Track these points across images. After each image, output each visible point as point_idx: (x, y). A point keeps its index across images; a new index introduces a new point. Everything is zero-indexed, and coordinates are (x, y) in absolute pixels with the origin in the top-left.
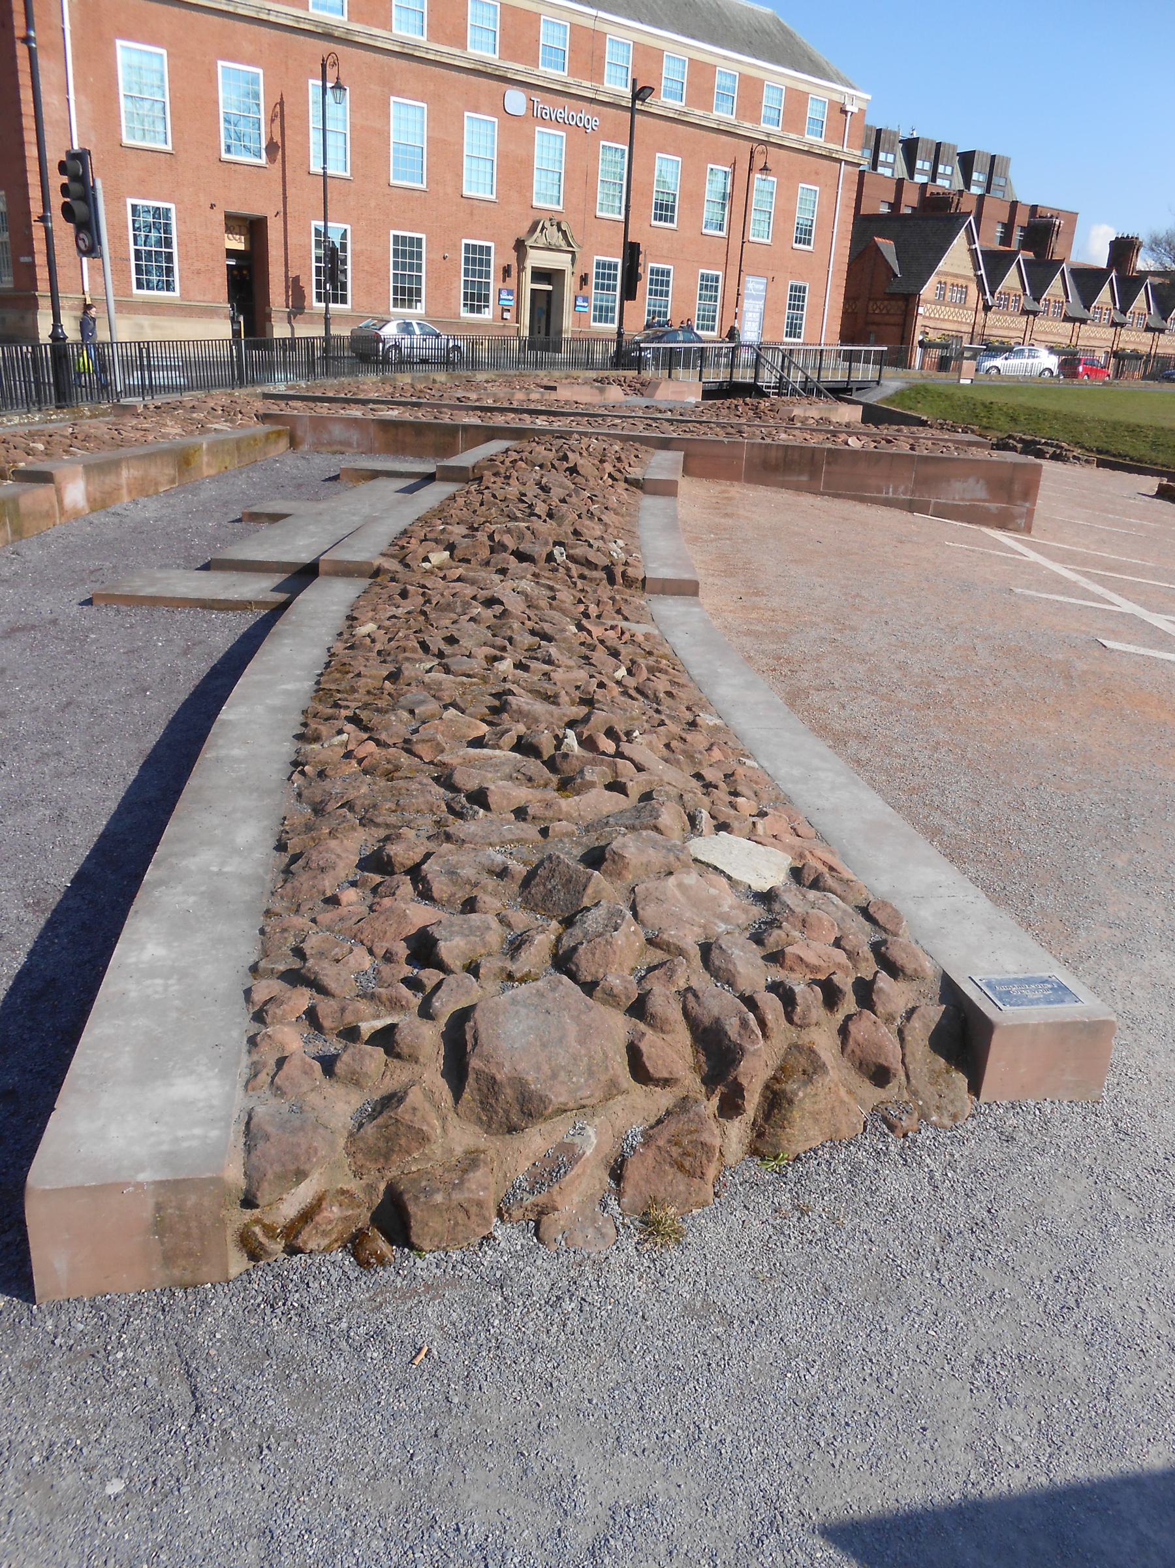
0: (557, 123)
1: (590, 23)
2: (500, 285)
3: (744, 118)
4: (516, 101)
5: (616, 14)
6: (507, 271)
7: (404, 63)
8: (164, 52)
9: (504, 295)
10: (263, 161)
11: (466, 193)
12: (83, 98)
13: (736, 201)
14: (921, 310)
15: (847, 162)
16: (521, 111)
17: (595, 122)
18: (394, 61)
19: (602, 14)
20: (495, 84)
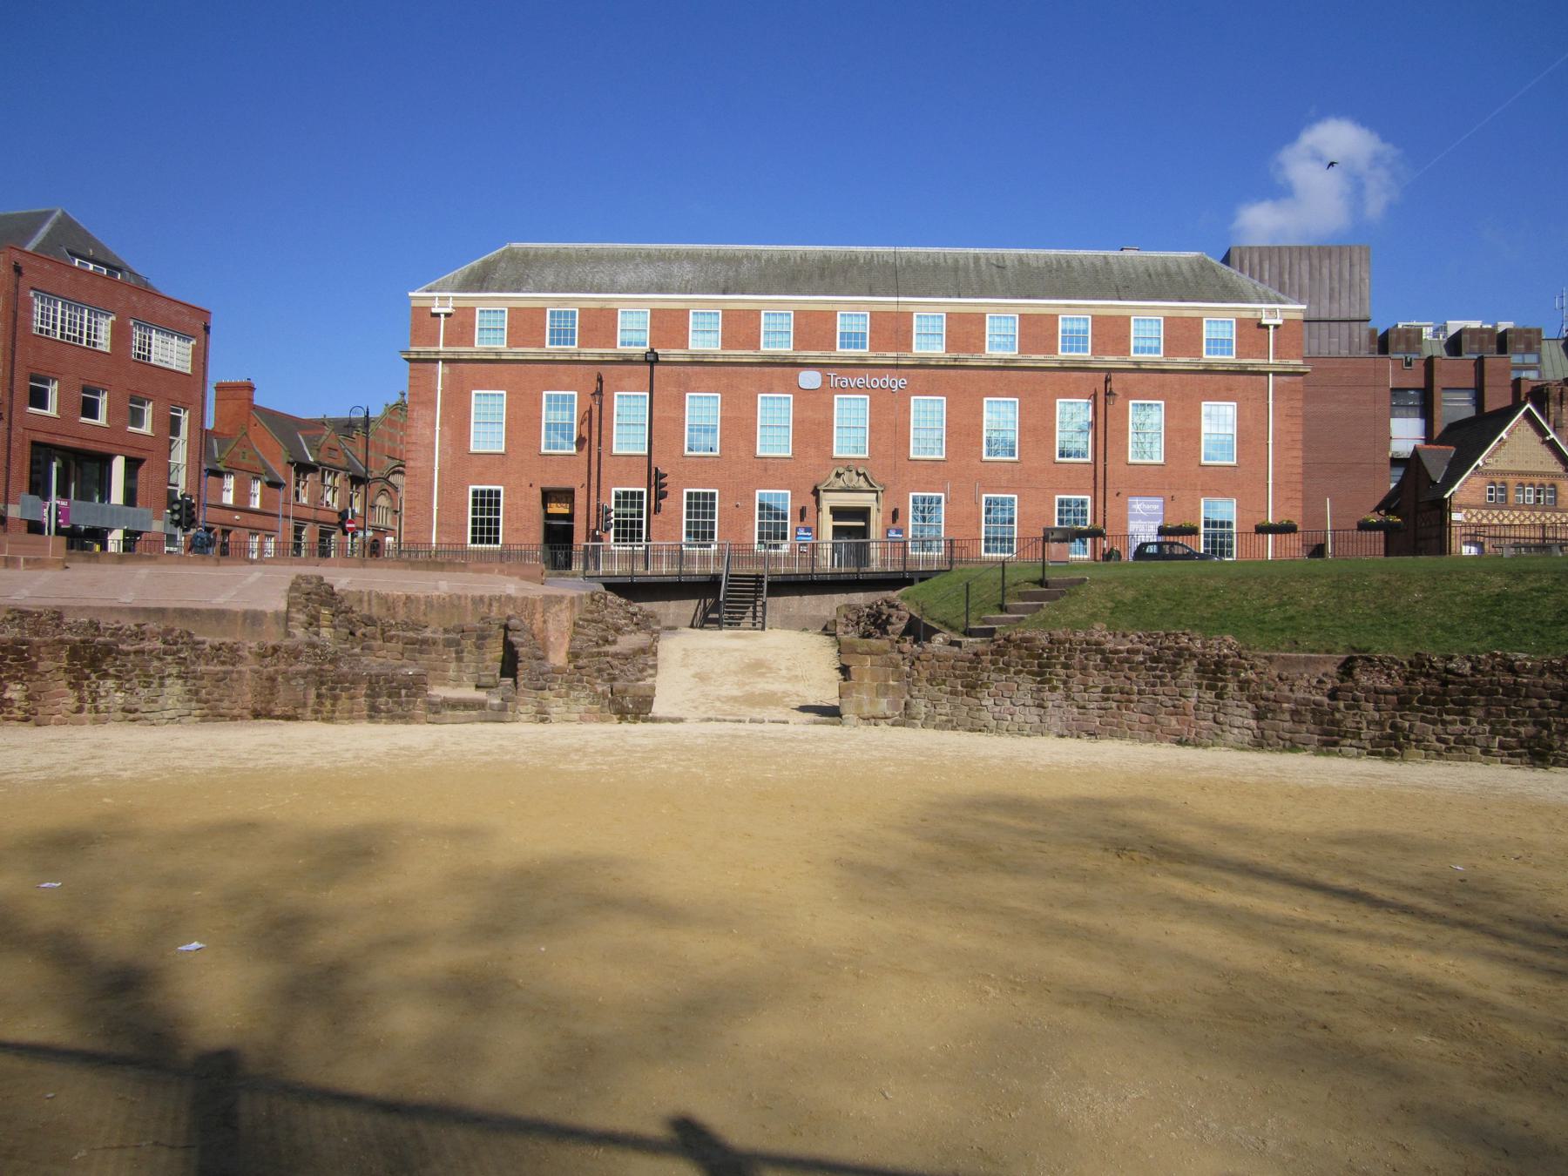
0: (858, 390)
1: (893, 308)
2: (798, 524)
3: (1105, 353)
4: (810, 379)
5: (930, 295)
6: (803, 512)
7: (697, 368)
8: (545, 393)
9: (802, 532)
10: (574, 451)
11: (759, 453)
13: (1106, 429)
14: (1456, 516)
15: (1275, 374)
16: (817, 385)
17: (901, 382)
18: (689, 369)
19: (901, 299)
20: (788, 370)
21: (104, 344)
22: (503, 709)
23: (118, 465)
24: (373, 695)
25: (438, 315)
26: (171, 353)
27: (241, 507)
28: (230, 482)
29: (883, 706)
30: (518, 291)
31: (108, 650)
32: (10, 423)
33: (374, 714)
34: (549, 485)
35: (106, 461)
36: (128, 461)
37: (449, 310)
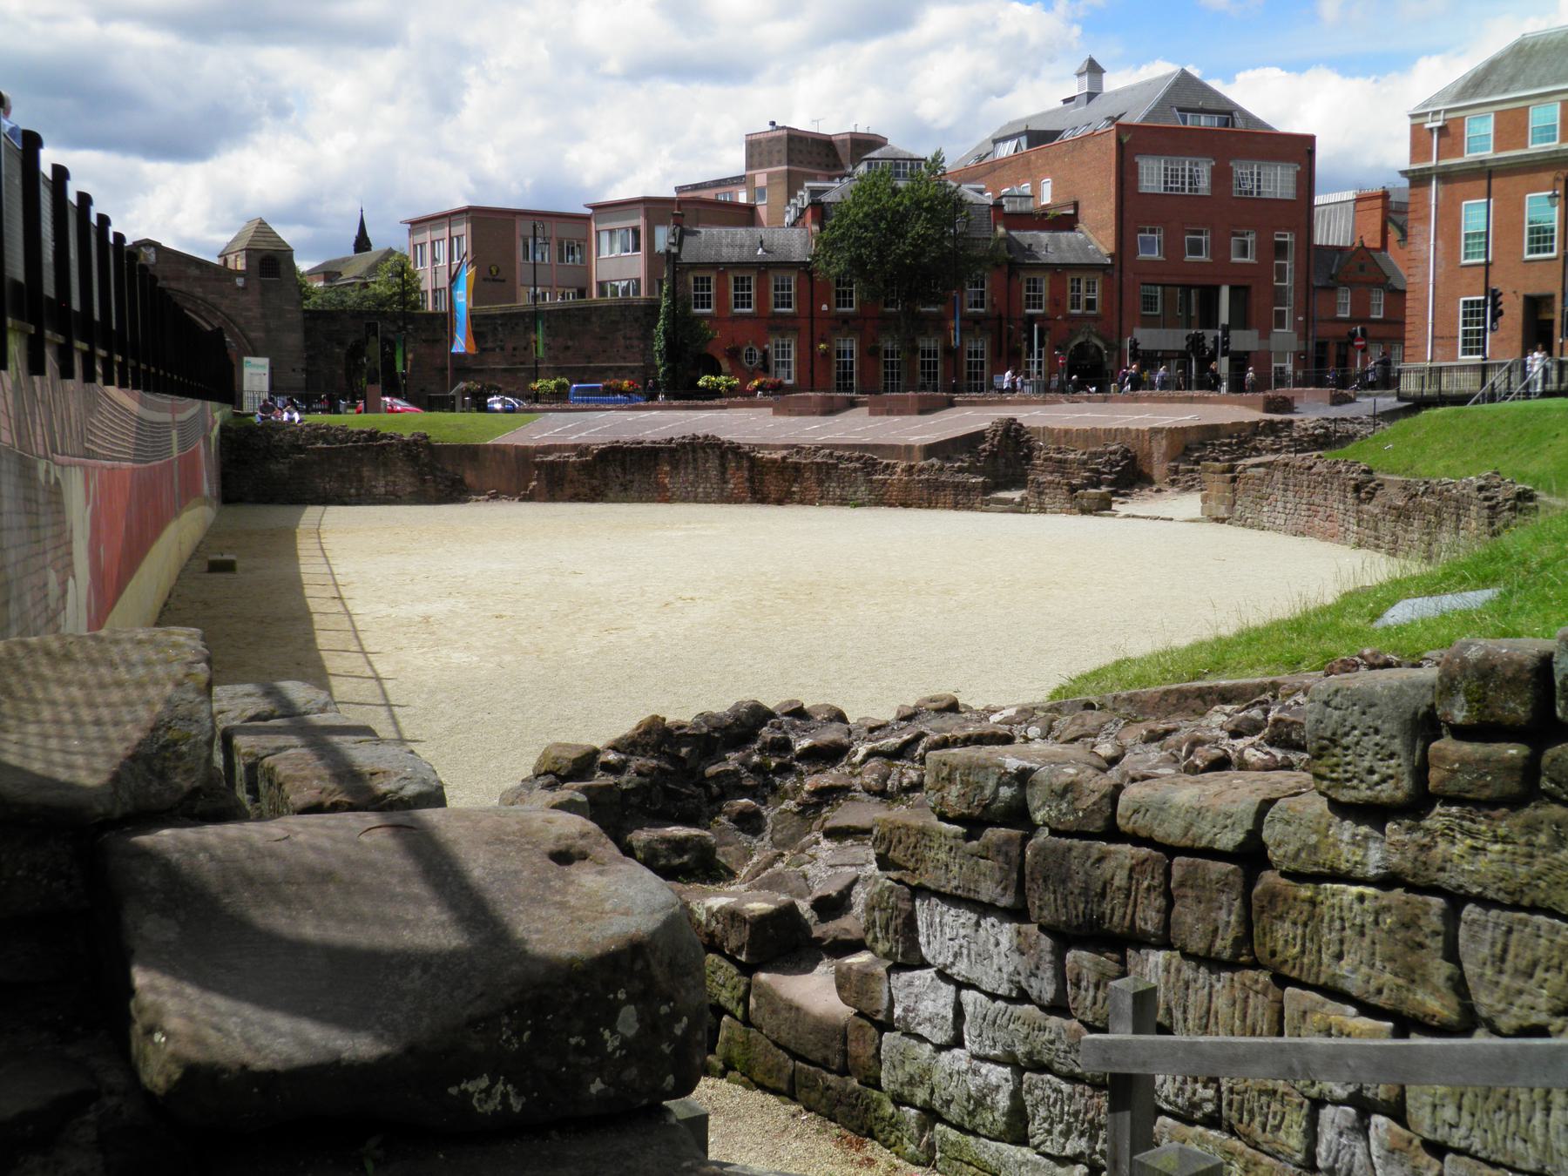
12: (1440, 242)
21: (1204, 185)
22: (1020, 504)
23: (1225, 292)
24: (956, 495)
25: (1431, 130)
26: (1277, 182)
27: (1360, 317)
28: (1345, 298)
29: (1222, 512)
30: (1506, 91)
31: (835, 466)
32: (1121, 271)
33: (956, 506)
34: (1529, 292)
35: (1217, 289)
36: (1233, 289)
37: (1439, 124)
